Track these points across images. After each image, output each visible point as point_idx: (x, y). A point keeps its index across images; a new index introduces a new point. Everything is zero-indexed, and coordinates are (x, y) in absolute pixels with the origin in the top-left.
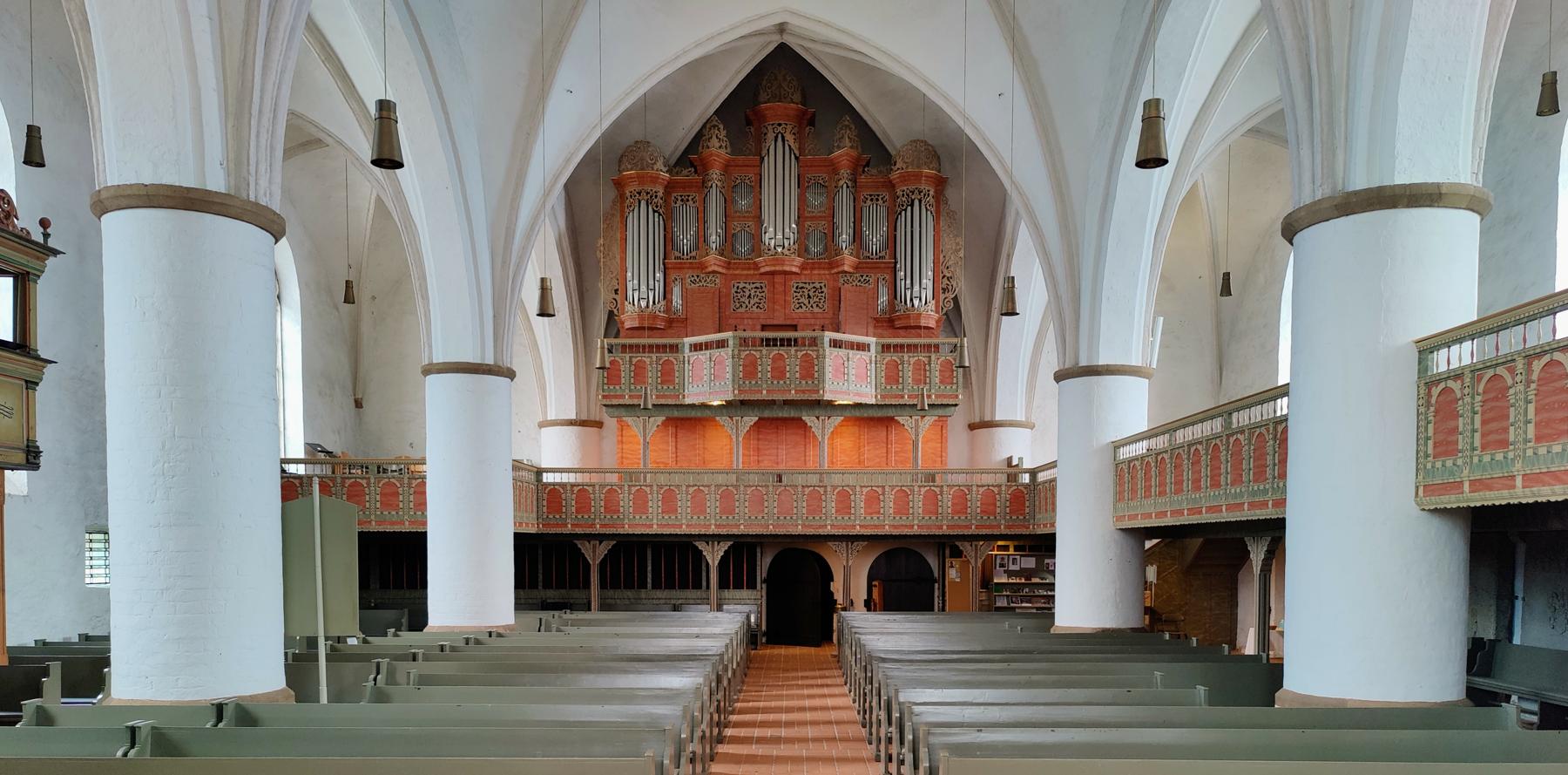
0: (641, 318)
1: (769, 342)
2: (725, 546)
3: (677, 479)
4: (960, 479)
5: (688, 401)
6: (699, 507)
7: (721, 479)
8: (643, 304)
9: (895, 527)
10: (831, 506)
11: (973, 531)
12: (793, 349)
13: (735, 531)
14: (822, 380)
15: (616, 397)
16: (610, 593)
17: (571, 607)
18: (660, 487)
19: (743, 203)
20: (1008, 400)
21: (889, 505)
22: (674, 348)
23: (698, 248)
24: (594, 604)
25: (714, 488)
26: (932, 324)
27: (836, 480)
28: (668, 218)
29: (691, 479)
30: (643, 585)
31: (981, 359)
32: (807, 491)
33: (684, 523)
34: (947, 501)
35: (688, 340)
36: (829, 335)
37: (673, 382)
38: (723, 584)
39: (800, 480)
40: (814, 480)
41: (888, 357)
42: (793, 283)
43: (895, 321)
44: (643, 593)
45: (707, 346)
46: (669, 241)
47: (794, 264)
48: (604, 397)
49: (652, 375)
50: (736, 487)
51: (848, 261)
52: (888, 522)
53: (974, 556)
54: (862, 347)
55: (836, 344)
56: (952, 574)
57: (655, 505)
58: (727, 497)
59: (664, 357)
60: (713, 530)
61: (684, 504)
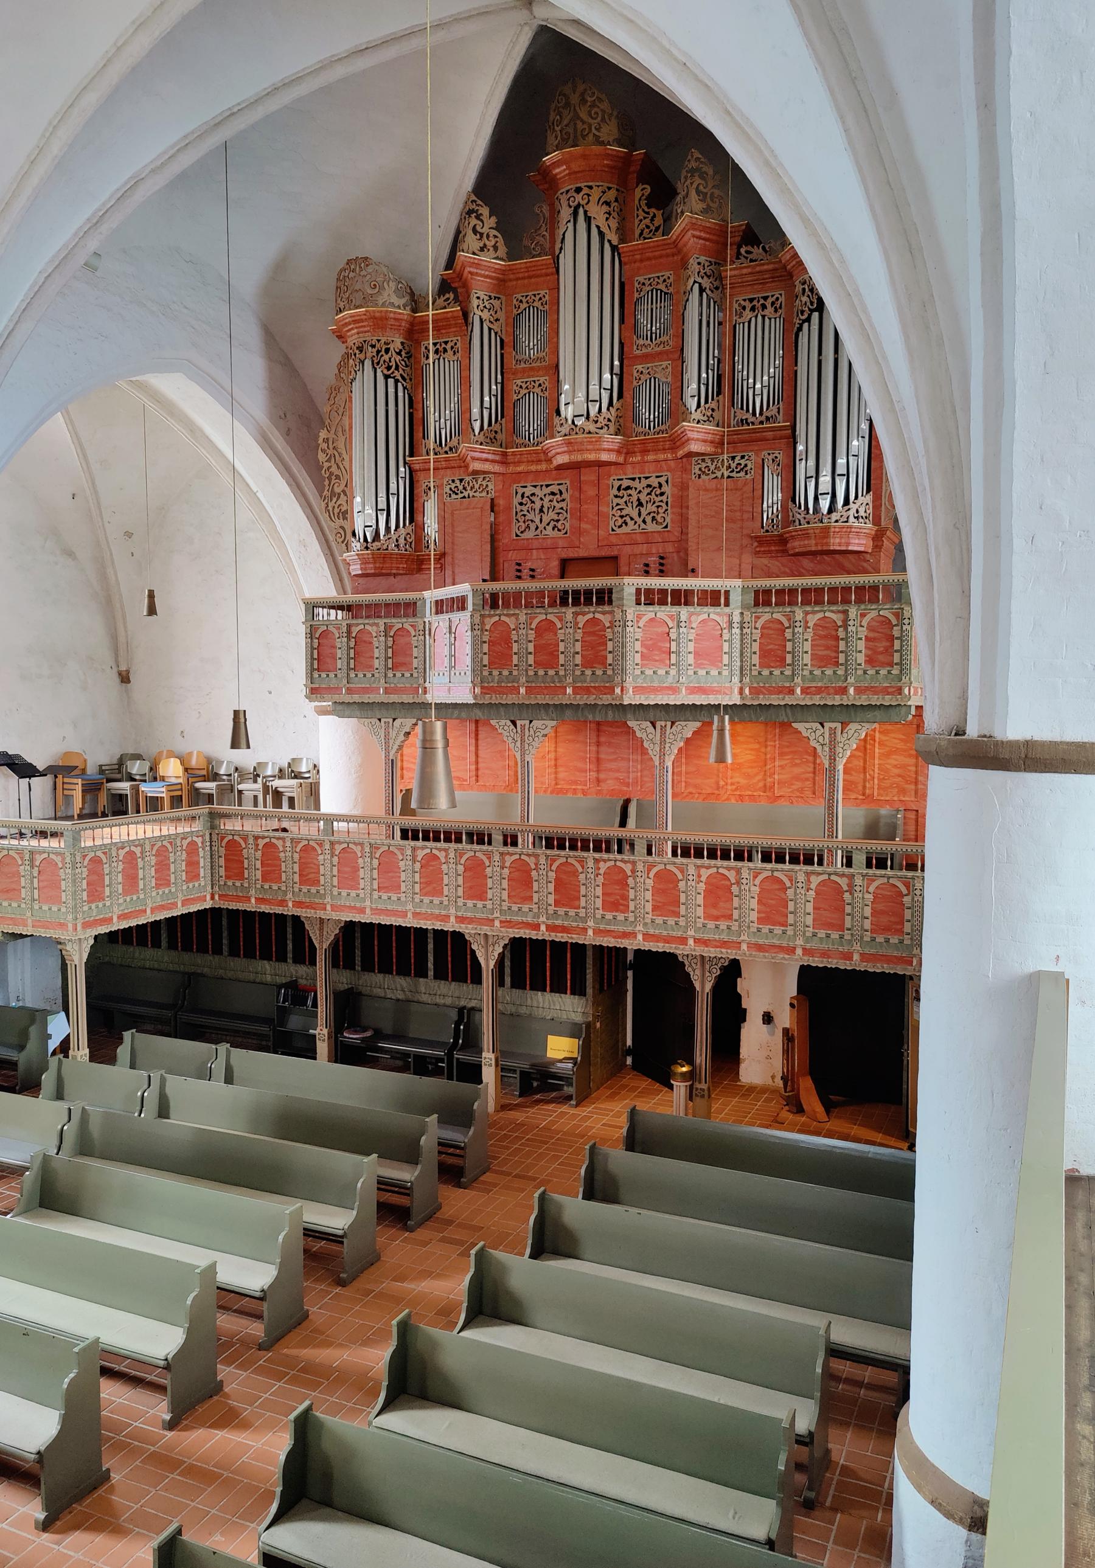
12: (569, 612)
19: (530, 344)
41: (766, 615)
51: (697, 433)
54: (713, 598)
55: (649, 598)
59: (397, 623)
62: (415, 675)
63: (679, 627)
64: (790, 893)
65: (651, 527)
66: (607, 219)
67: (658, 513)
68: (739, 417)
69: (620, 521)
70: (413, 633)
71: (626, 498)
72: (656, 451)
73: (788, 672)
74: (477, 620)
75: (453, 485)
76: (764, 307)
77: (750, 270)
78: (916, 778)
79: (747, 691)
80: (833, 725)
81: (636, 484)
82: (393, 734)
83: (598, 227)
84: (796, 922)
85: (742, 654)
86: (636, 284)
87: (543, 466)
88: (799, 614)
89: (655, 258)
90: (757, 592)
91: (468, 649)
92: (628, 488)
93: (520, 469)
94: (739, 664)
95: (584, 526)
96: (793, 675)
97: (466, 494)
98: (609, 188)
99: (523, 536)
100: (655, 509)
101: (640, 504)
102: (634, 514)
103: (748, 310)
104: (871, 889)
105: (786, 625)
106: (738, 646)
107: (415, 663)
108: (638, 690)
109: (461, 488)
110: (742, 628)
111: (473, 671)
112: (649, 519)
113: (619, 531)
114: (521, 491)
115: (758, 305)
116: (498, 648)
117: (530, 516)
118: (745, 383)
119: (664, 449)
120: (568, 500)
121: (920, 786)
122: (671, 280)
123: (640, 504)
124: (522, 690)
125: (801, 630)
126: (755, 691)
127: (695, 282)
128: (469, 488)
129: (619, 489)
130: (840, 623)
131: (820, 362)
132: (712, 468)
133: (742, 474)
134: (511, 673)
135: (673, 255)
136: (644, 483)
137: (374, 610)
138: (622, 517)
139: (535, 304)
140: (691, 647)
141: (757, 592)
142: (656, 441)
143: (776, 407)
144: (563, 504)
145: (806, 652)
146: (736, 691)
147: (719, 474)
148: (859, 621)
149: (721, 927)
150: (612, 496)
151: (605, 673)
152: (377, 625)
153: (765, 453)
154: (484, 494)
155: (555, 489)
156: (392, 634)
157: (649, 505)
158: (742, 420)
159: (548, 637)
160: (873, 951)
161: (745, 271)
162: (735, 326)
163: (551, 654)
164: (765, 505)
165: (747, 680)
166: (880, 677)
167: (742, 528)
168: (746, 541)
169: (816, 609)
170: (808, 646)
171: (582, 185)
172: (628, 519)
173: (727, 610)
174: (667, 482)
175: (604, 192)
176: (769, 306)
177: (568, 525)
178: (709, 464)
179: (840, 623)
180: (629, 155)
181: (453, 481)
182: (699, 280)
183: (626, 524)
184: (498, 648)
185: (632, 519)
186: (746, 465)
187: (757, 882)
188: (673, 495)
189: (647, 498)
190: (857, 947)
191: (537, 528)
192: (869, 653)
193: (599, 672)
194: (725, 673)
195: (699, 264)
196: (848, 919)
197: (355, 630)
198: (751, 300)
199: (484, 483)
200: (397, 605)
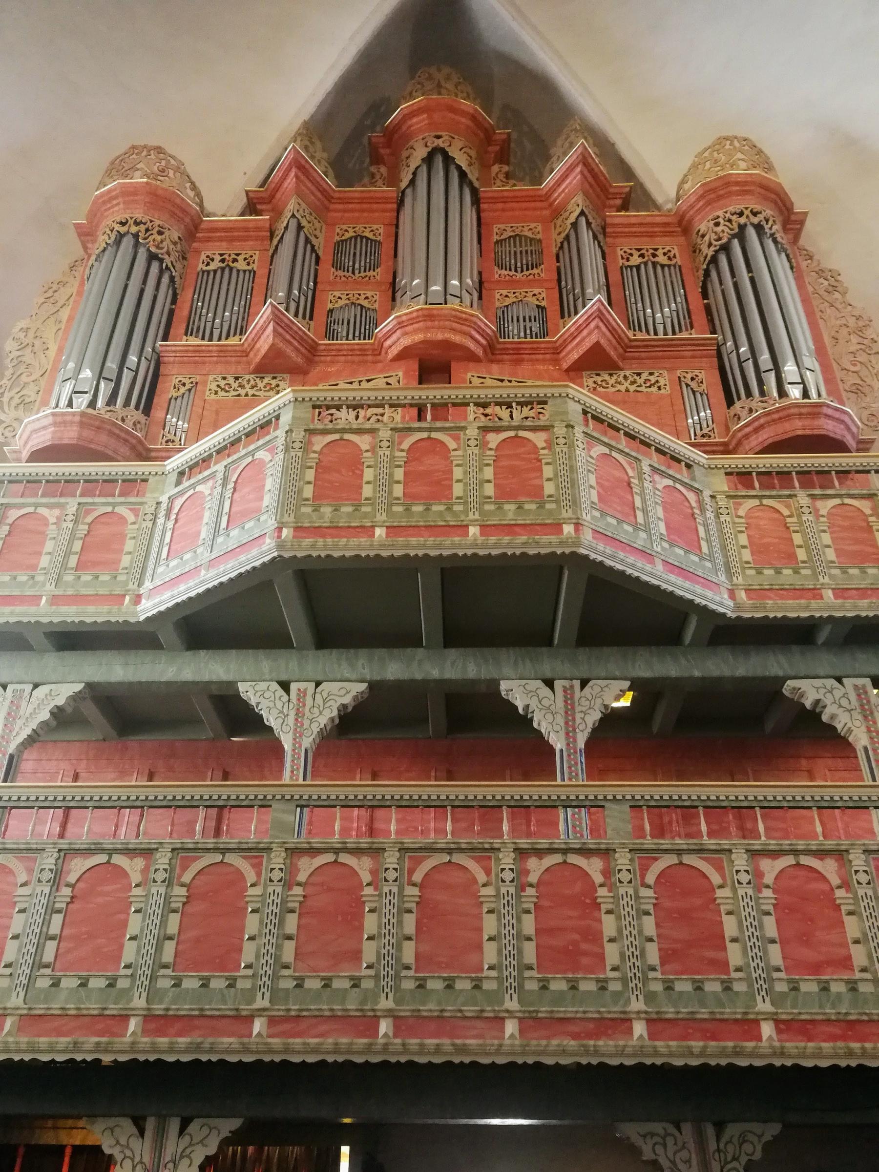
0: (60, 421)
37: (113, 565)
59: (101, 505)
63: (640, 479)
74: (299, 435)
82: (26, 709)
91: (271, 483)
107: (126, 560)
110: (718, 515)
119: (544, 360)
133: (654, 389)
135: (541, 209)
147: (622, 388)
152: (61, 506)
153: (678, 373)
159: (431, 462)
200: (110, 481)
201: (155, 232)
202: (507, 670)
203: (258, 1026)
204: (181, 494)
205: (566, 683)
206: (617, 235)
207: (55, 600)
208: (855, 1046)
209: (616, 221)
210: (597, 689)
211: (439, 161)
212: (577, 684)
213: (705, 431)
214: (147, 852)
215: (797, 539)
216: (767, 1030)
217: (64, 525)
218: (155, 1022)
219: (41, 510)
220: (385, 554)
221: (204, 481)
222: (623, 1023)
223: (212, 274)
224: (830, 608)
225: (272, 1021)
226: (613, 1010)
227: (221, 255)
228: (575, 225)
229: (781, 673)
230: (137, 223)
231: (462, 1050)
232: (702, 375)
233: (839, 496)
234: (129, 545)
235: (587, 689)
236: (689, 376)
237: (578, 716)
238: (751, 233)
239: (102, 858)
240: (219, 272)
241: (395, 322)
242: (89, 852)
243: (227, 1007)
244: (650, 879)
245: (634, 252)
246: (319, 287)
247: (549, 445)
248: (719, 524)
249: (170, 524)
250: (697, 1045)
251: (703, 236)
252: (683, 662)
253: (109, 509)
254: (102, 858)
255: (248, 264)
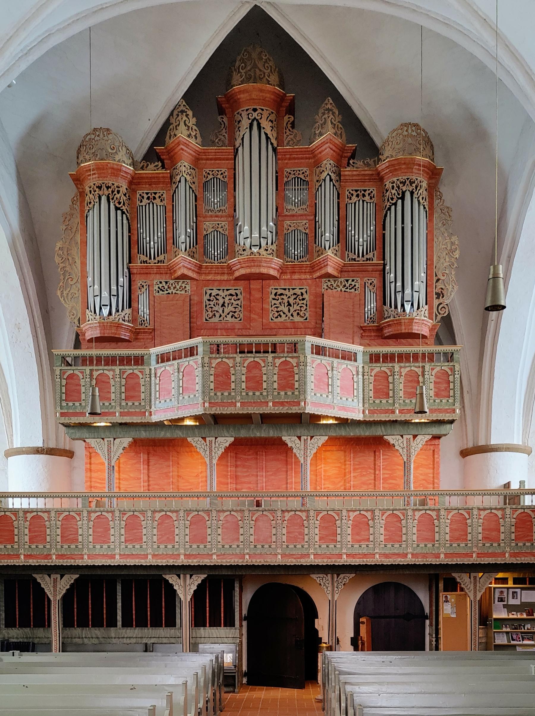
1: (244, 349)
2: (198, 579)
3: (141, 504)
4: (455, 502)
5: (155, 418)
6: (167, 534)
7: (190, 503)
8: (106, 311)
9: (386, 556)
10: (314, 531)
11: (474, 560)
13: (207, 562)
14: (303, 391)
15: (75, 414)
16: (77, 631)
17: (25, 647)
18: (123, 512)
20: (505, 422)
21: (379, 530)
22: (139, 361)
23: (165, 251)
24: (56, 644)
25: (188, 516)
26: (425, 331)
27: (320, 503)
28: (133, 219)
29: (158, 504)
30: (112, 623)
31: (474, 379)
32: (287, 516)
33: (148, 552)
34: (445, 528)
35: (155, 351)
36: (311, 340)
37: (138, 398)
38: (198, 621)
39: (280, 504)
40: (295, 503)
41: (378, 368)
42: (272, 288)
43: (384, 331)
44: (112, 632)
45: (177, 355)
46: (134, 244)
47: (272, 265)
48: (62, 414)
49: (115, 389)
50: (208, 512)
52: (378, 550)
53: (474, 588)
56: (447, 609)
57: (117, 533)
58: (198, 522)
59: (129, 369)
60: (182, 561)
61: (149, 531)
62: (143, 404)
64: (403, 522)
65: (297, 319)
66: (271, 130)
67: (301, 311)
68: (350, 257)
69: (277, 314)
70: (141, 376)
71: (280, 300)
72: (300, 273)
73: (391, 401)
75: (160, 285)
76: (364, 196)
77: (357, 173)
78: (433, 481)
79: (367, 412)
80: (408, 437)
81: (286, 292)
83: (266, 134)
84: (407, 539)
85: (363, 390)
86: (285, 173)
87: (225, 277)
88: (397, 369)
89: (298, 158)
90: (371, 355)
92: (281, 294)
93: (209, 278)
94: (362, 396)
95: (253, 316)
96: (394, 402)
97: (170, 291)
98: (272, 113)
99: (211, 320)
100: (299, 309)
101: (289, 305)
102: (286, 310)
103: (354, 196)
104: (449, 517)
105: (389, 374)
106: (362, 386)
107: (143, 396)
108: (314, 404)
109: (166, 287)
110: (363, 375)
111: (203, 392)
112: (295, 314)
113: (275, 320)
114: (209, 292)
115: (361, 194)
116: (220, 379)
117: (215, 308)
118: (353, 238)
120: (242, 299)
121: (436, 485)
122: (308, 173)
123: (289, 305)
124: (238, 404)
125: (398, 377)
126: (371, 412)
127: (328, 174)
128: (172, 288)
129: (276, 295)
130: (420, 373)
131: (403, 228)
132: (335, 285)
133: (353, 290)
134: (230, 394)
136: (292, 292)
137: (110, 361)
138: (278, 312)
139: (218, 177)
140: (338, 383)
141: (371, 355)
142: (301, 267)
143: (372, 253)
144: (239, 302)
145: (401, 390)
146: (361, 411)
147: (339, 289)
148: (431, 371)
149: (363, 546)
150: (271, 299)
151: (293, 393)
154: (183, 292)
155: (233, 292)
156: (125, 377)
157: (295, 305)
158: (352, 259)
159: (255, 372)
160: (452, 551)
161: (355, 173)
162: (347, 204)
163: (258, 382)
164: (366, 309)
165: (366, 406)
166: (443, 404)
167: (354, 321)
168: (356, 329)
169: (407, 365)
170: (401, 386)
171: (258, 107)
172: (281, 313)
173: (356, 364)
174: (306, 292)
175: (270, 114)
176: (367, 195)
177: (242, 315)
178: (333, 283)
179: (420, 373)
180: (285, 95)
181: (161, 283)
182: (330, 173)
183: (281, 316)
184: (220, 379)
185: (284, 313)
186: (355, 285)
187: (384, 518)
188: (309, 300)
189: (294, 301)
190: (442, 550)
191: (220, 316)
192: (436, 390)
193: (289, 393)
194: (355, 401)
195: (330, 164)
196: (437, 535)
197: (95, 374)
198: (356, 191)
199: (183, 285)
201: (116, 192)
202: (284, 433)
203: (214, 557)
204: (161, 367)
205: (306, 438)
206: (346, 181)
207: (122, 414)
208: (365, 560)
209: (347, 173)
210: (316, 440)
211: (255, 123)
212: (309, 438)
213: (372, 316)
214: (177, 512)
215: (391, 386)
216: (345, 556)
217: (116, 380)
218: (187, 556)
219: (105, 372)
220: (241, 412)
221: (170, 366)
222: (308, 555)
223: (144, 207)
224: (397, 417)
225: (217, 556)
226: (306, 552)
227: (147, 194)
228: (325, 180)
229: (381, 434)
230: (108, 188)
231: (267, 562)
232: (375, 282)
233: (411, 367)
234: (143, 389)
235: (313, 440)
236: (369, 282)
237: (309, 451)
238: (408, 195)
239: (164, 513)
240: (147, 205)
241: (237, 261)
242: (160, 511)
243: (205, 553)
244: (319, 518)
245: (354, 192)
246: (198, 218)
247: (298, 365)
248: (363, 379)
249: (157, 382)
250: (325, 560)
251: (387, 191)
252: (348, 429)
253: (132, 371)
254: (164, 513)
255: (161, 201)
